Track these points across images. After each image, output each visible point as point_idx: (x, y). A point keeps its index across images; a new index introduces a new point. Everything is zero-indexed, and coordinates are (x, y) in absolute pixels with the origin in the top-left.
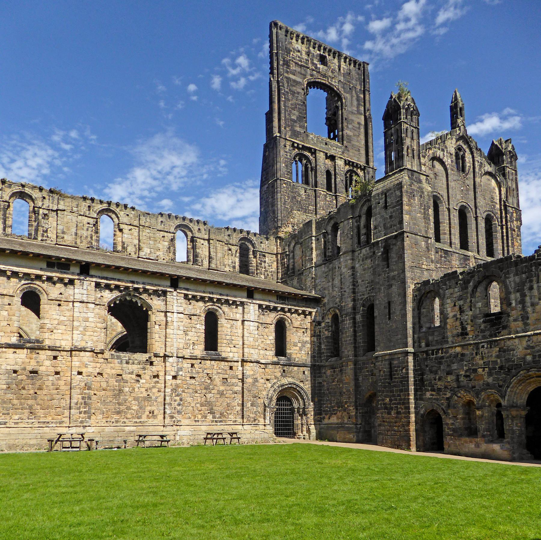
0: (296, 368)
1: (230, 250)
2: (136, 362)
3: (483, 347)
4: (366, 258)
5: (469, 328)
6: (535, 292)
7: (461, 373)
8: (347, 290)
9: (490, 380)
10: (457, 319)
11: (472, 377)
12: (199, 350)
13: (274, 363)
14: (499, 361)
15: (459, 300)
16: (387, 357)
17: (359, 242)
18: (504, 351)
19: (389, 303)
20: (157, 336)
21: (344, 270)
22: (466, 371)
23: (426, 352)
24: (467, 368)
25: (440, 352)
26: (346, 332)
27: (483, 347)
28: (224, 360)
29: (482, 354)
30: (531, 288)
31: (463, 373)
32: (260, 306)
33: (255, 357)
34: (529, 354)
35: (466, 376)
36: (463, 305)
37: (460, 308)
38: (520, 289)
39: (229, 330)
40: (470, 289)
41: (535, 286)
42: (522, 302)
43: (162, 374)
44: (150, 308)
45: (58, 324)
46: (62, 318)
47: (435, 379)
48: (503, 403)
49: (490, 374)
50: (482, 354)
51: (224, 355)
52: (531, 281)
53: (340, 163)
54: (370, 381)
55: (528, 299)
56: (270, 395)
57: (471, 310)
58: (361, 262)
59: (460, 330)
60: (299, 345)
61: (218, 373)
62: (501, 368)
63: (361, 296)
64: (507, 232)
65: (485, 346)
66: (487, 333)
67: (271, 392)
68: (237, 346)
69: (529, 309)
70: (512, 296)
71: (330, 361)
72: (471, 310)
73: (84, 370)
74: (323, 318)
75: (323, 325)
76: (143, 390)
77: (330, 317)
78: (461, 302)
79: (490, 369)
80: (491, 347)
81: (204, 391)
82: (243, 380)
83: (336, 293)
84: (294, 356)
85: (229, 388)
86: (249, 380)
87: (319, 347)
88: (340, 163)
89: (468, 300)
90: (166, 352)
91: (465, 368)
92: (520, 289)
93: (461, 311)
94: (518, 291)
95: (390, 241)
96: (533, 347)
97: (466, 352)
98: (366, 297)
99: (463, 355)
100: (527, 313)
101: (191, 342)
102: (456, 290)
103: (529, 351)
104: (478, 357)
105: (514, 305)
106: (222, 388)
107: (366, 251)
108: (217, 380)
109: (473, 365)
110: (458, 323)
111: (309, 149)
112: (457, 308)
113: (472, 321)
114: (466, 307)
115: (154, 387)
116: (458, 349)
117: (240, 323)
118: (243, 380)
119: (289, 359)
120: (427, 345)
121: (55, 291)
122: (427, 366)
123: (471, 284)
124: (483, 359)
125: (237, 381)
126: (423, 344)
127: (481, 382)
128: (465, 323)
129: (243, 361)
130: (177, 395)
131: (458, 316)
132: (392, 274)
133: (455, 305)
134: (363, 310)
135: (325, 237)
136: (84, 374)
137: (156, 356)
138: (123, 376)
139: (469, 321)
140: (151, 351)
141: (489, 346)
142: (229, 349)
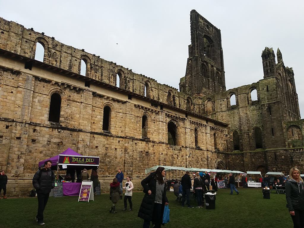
0: (221, 154)
1: (185, 102)
2: (177, 149)
4: (254, 110)
8: (245, 123)
12: (194, 146)
13: (215, 152)
16: (273, 151)
17: (248, 104)
19: (272, 129)
20: (182, 138)
21: (241, 114)
23: (294, 150)
25: (301, 150)
26: (244, 140)
28: (201, 150)
32: (210, 127)
33: (210, 149)
39: (202, 137)
43: (184, 155)
44: (179, 125)
45: (154, 131)
46: (155, 129)
47: (300, 161)
51: (201, 148)
53: (215, 69)
54: (260, 161)
56: (215, 166)
58: (251, 112)
60: (221, 144)
61: (200, 156)
63: (251, 125)
64: (296, 103)
67: (216, 165)
68: (204, 144)
71: (234, 152)
73: (163, 152)
74: (228, 133)
75: (229, 136)
76: (179, 162)
77: (232, 133)
81: (196, 164)
82: (207, 160)
83: (237, 123)
84: (220, 149)
85: (203, 162)
86: (209, 159)
87: (227, 145)
88: (215, 69)
90: (186, 145)
95: (271, 105)
98: (254, 126)
101: (192, 141)
106: (201, 162)
107: (253, 107)
108: (200, 160)
111: (206, 62)
115: (182, 161)
117: (204, 134)
118: (207, 160)
119: (219, 150)
120: (293, 146)
121: (153, 116)
122: (294, 155)
125: (205, 159)
126: (291, 146)
129: (207, 150)
130: (190, 165)
132: (273, 118)
134: (253, 131)
135: (227, 100)
136: (163, 154)
137: (183, 147)
138: (174, 155)
140: (180, 145)
142: (202, 145)
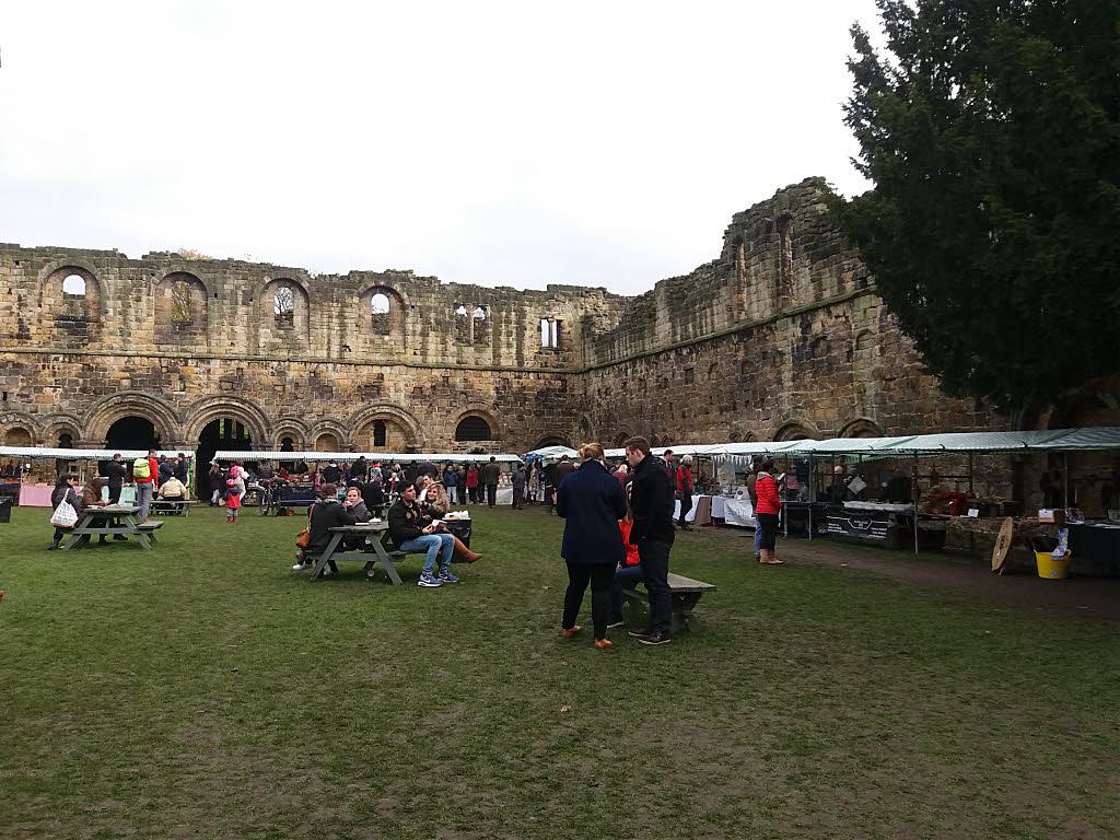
3: (57, 359)
5: (33, 329)
6: (143, 304)
7: (11, 391)
9: (65, 404)
10: (12, 313)
11: (32, 397)
14: (81, 381)
15: (17, 287)
18: (91, 369)
22: (23, 388)
24: (25, 384)
27: (57, 359)
29: (53, 368)
30: (138, 300)
31: (17, 391)
34: (127, 378)
35: (22, 396)
36: (25, 296)
37: (20, 299)
38: (123, 295)
40: (40, 277)
41: (144, 298)
42: (124, 313)
48: (82, 436)
49: (65, 396)
50: (53, 368)
52: (140, 291)
55: (132, 311)
57: (40, 306)
59: (17, 331)
62: (84, 390)
65: (61, 359)
66: (65, 342)
69: (133, 324)
70: (110, 303)
72: (40, 306)
78: (23, 292)
79: (65, 390)
80: (70, 362)
89: (37, 291)
91: (20, 384)
92: (123, 295)
93: (21, 302)
94: (119, 298)
96: (133, 370)
97: (23, 361)
99: (17, 365)
100: (129, 328)
102: (15, 272)
103: (128, 374)
104: (47, 371)
105: (111, 314)
109: (36, 381)
110: (13, 319)
112: (14, 297)
113: (40, 321)
114: (31, 300)
116: (10, 356)
123: (45, 270)
124: (54, 376)
127: (49, 406)
128: (26, 322)
131: (15, 310)
133: (10, 293)
139: (35, 321)
141: (67, 360)
